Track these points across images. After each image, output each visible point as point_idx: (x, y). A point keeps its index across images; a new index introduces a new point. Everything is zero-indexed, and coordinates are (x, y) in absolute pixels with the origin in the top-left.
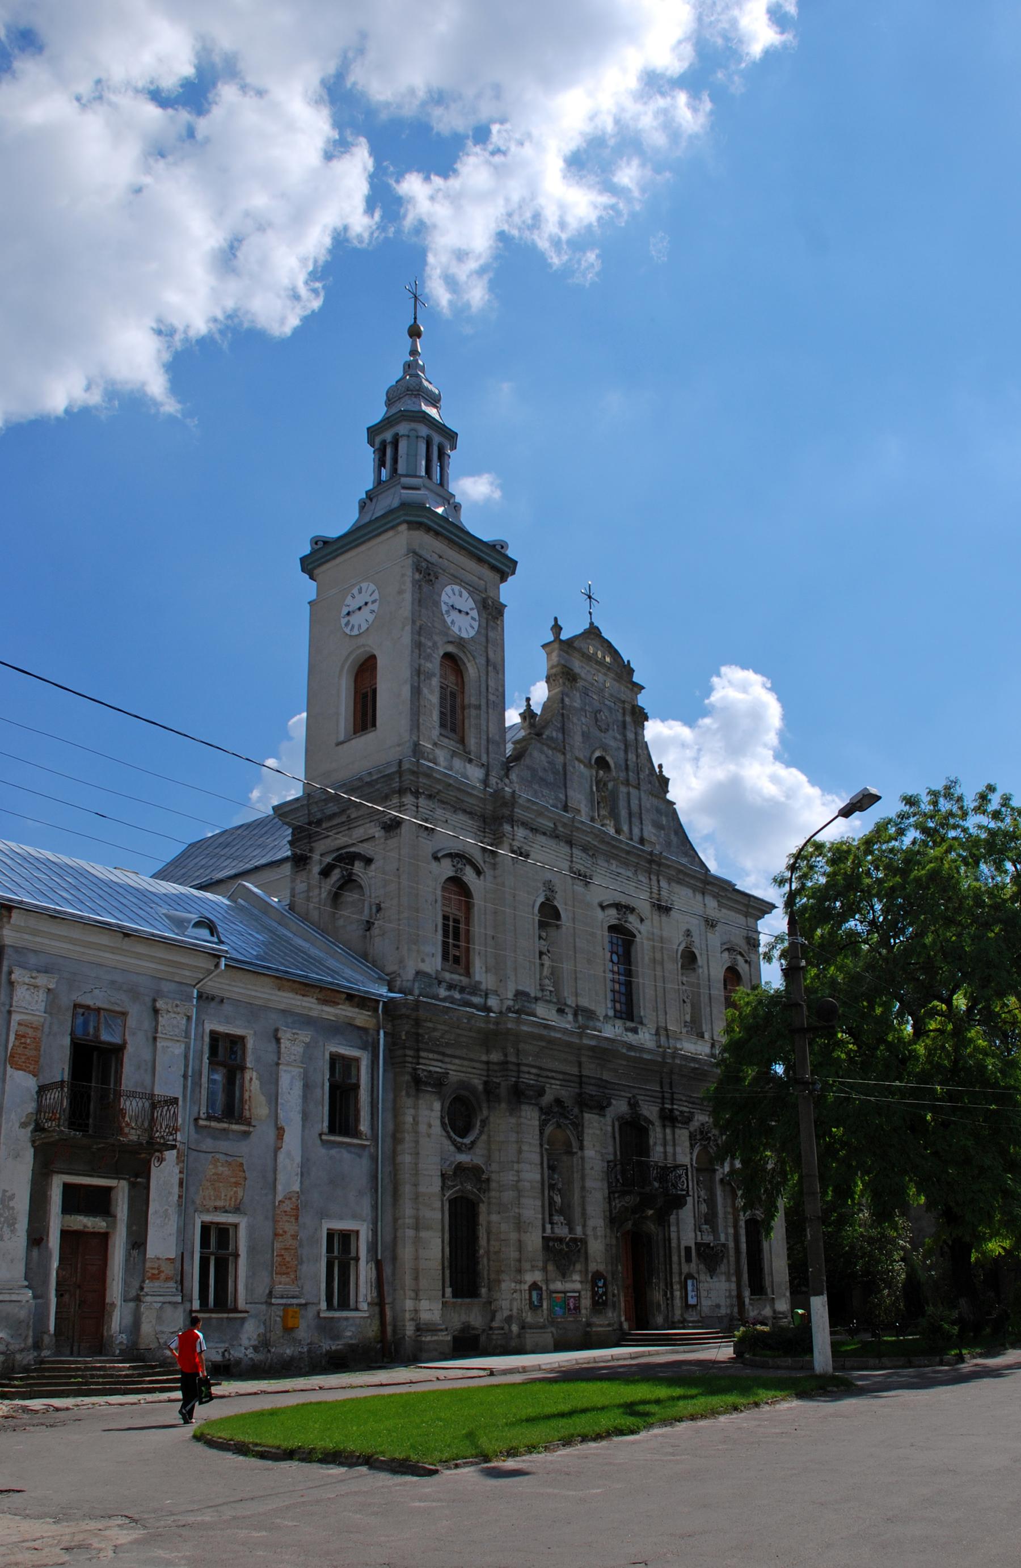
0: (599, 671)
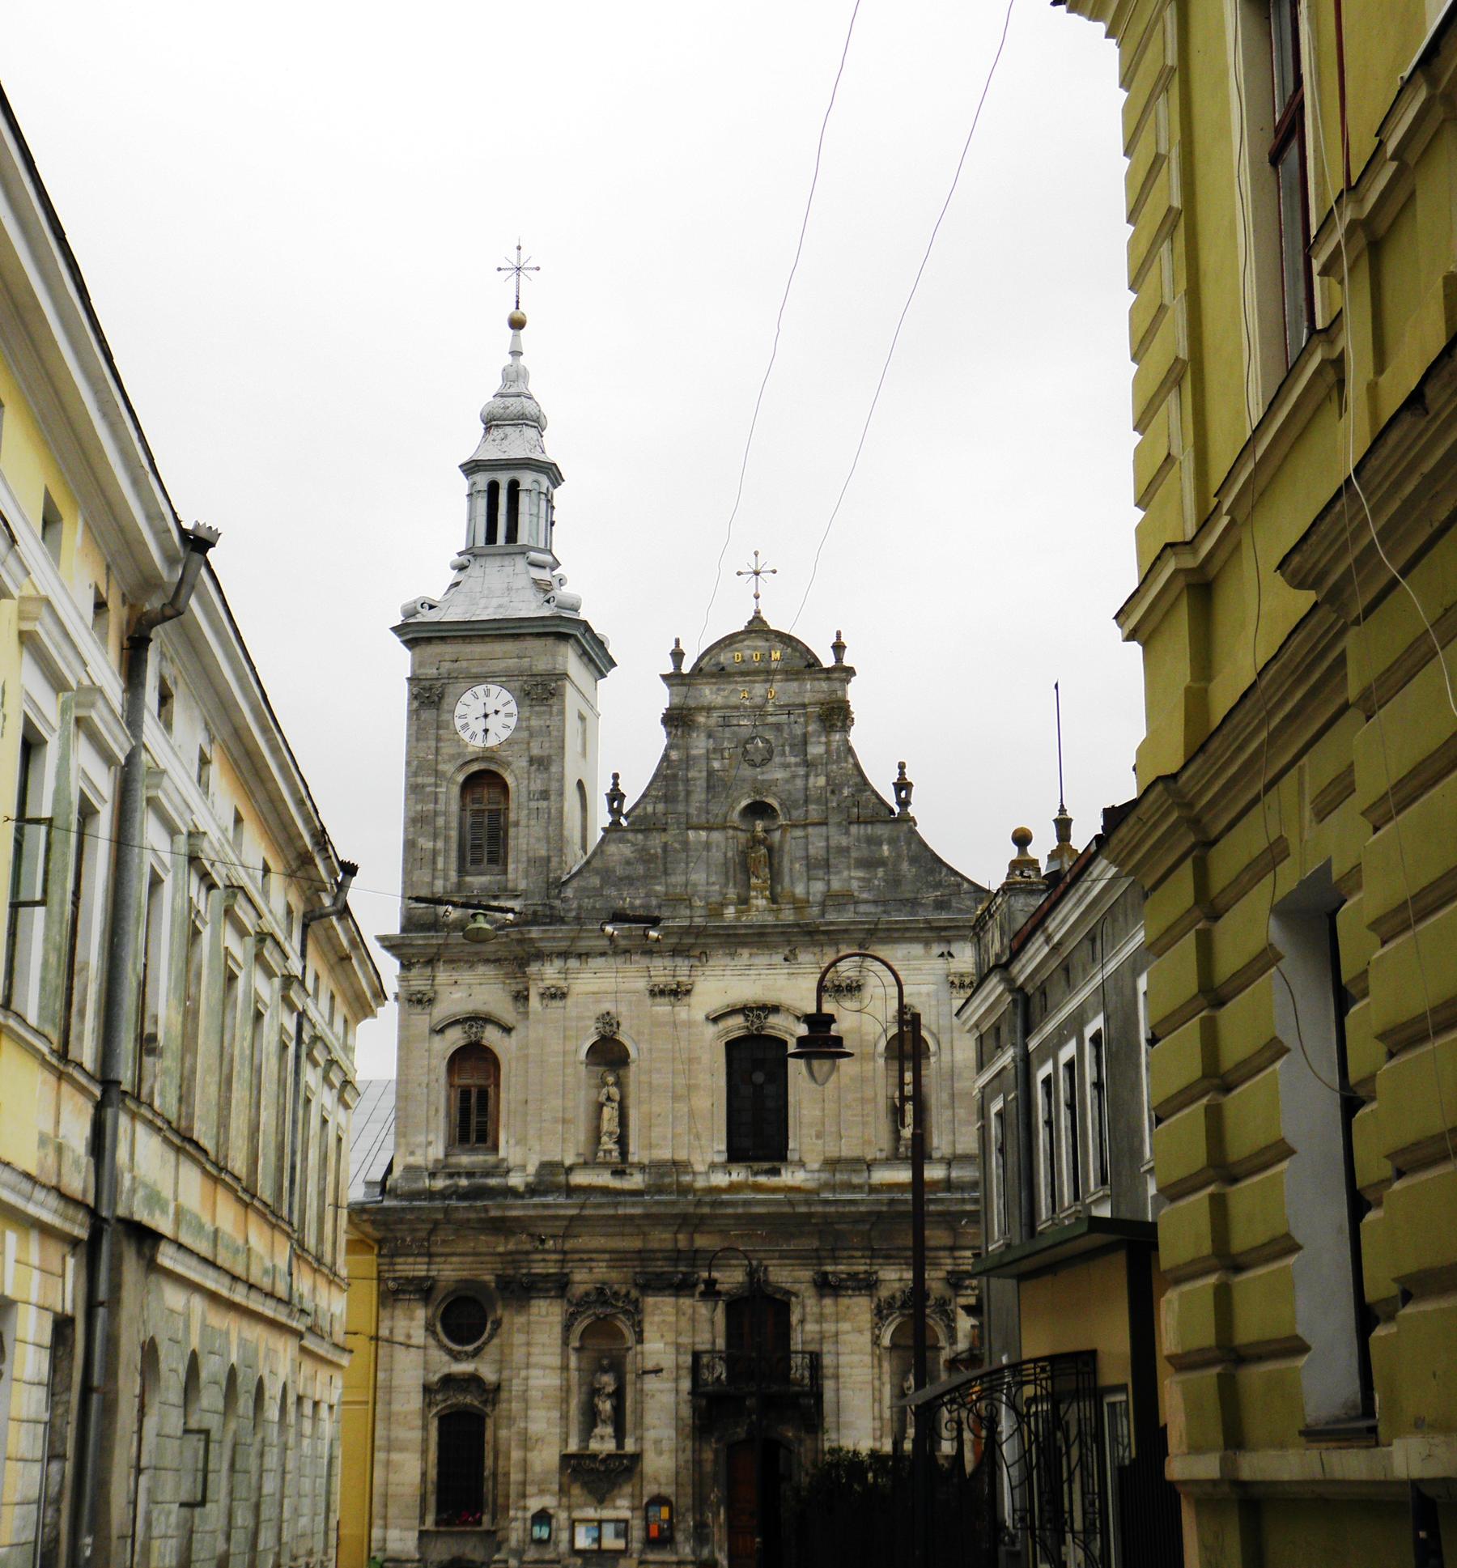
0: (754, 682)
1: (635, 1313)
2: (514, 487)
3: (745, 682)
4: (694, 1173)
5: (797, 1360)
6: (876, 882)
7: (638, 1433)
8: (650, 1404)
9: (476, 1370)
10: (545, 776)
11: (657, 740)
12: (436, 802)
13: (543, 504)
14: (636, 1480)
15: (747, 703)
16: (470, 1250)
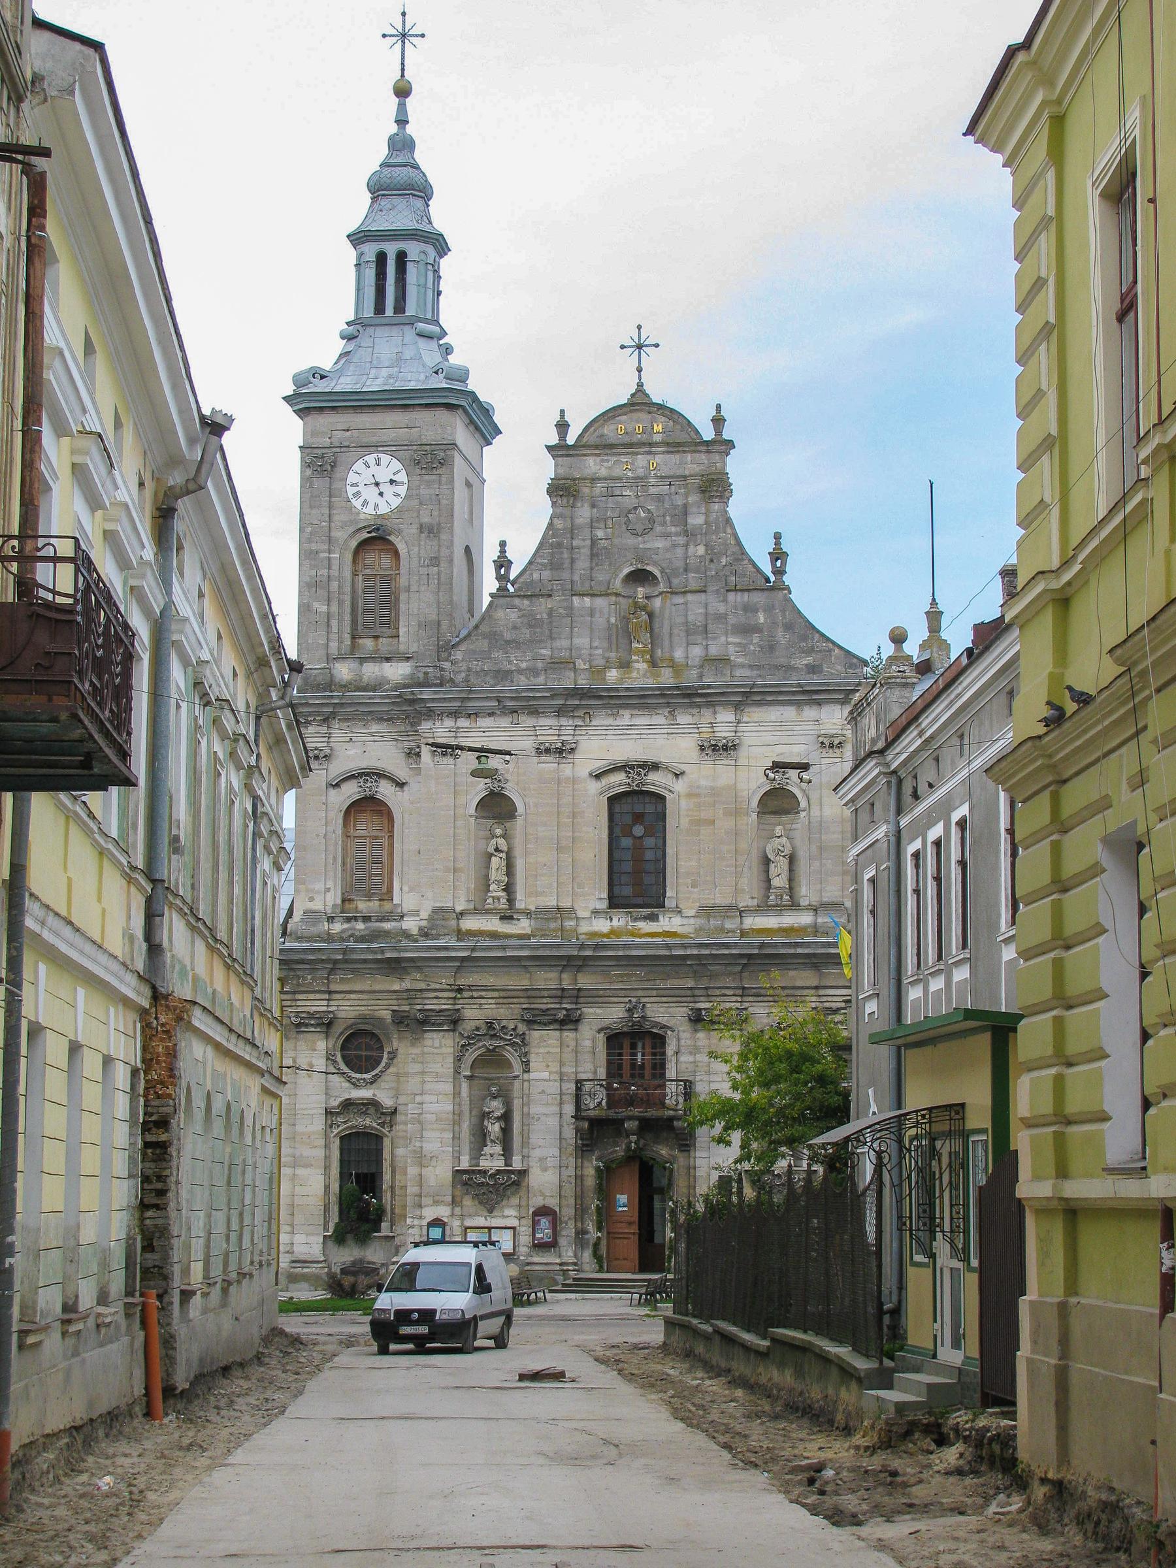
0: (637, 454)
1: (522, 1043)
2: (401, 257)
3: (628, 454)
4: (577, 918)
5: (671, 1088)
6: (752, 648)
7: (525, 1151)
8: (536, 1127)
10: (435, 543)
11: (543, 509)
13: (430, 274)
14: (523, 1192)
15: (630, 474)
16: (367, 988)
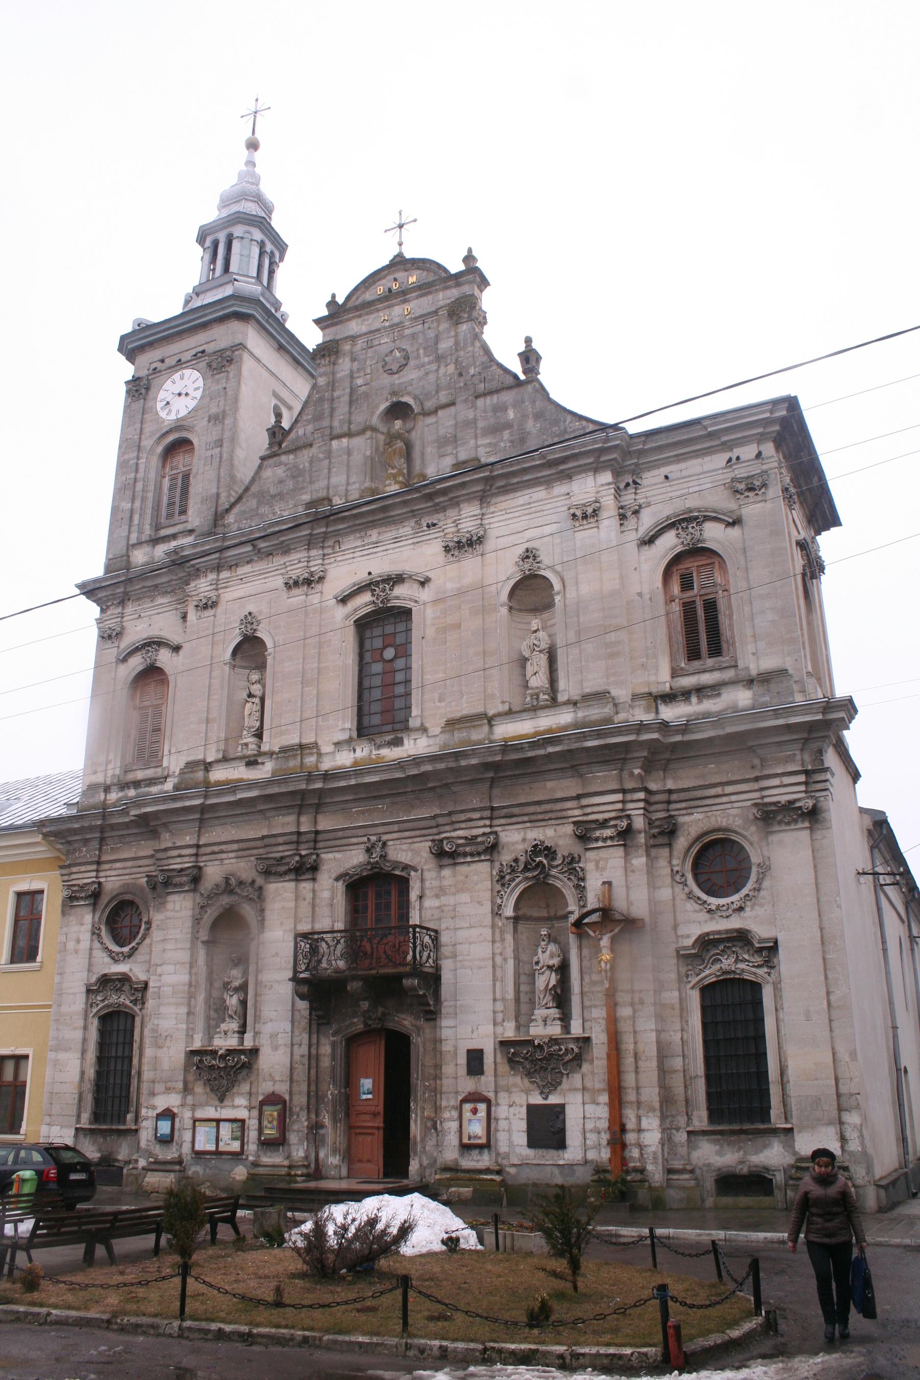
0: (394, 305)
6: (502, 444)
9: (131, 970)
10: (220, 427)
12: (137, 471)
15: (387, 324)
16: (133, 856)
